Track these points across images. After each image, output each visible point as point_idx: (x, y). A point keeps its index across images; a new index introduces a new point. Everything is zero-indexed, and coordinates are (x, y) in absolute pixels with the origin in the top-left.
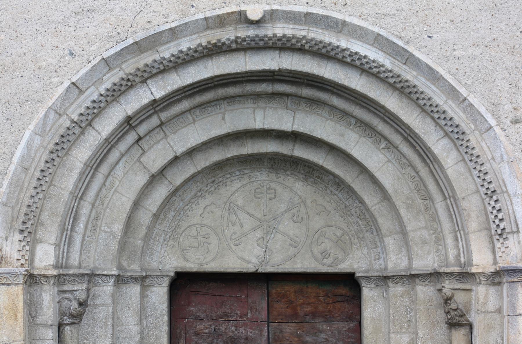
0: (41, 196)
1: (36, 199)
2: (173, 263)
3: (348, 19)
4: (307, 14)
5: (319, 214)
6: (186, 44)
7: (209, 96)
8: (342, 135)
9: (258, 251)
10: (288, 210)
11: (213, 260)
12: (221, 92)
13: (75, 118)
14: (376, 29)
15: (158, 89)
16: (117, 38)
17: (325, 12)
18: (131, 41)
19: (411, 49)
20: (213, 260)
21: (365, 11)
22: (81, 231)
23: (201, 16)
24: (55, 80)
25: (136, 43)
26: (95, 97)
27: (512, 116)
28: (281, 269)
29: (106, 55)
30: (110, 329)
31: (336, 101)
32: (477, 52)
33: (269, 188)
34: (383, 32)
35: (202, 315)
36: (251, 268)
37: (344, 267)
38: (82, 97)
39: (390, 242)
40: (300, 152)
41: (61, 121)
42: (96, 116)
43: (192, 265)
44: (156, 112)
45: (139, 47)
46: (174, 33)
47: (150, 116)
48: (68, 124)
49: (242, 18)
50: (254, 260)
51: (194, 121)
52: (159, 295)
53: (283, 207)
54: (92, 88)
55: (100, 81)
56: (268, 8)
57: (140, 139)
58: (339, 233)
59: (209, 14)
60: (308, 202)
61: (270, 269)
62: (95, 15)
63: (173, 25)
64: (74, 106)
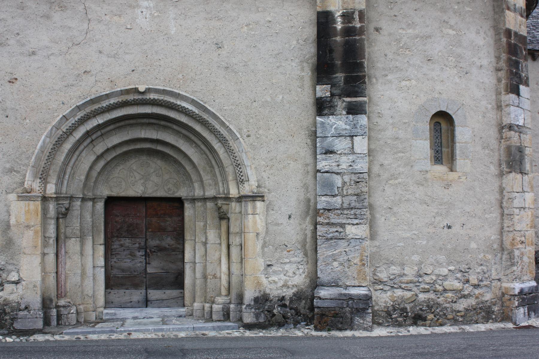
0: (49, 163)
1: (47, 165)
2: (106, 193)
3: (181, 93)
4: (164, 90)
5: (167, 173)
6: (112, 101)
7: (122, 123)
8: (177, 141)
9: (142, 188)
10: (154, 172)
11: (123, 192)
12: (127, 122)
13: (65, 131)
14: (192, 97)
15: (100, 120)
16: (83, 97)
17: (171, 90)
18: (89, 99)
19: (206, 105)
20: (123, 192)
21: (188, 89)
22: (67, 179)
23: (119, 89)
24: (56, 114)
25: (91, 100)
26: (73, 122)
27: (247, 134)
28: (151, 196)
29: (78, 104)
30: (79, 220)
31: (175, 127)
32: (233, 108)
33: (147, 163)
34: (195, 98)
35: (118, 214)
36: (139, 195)
37: (177, 195)
38: (68, 122)
39: (196, 185)
40: (160, 148)
41: (58, 132)
42: (74, 130)
43: (114, 194)
44: (99, 130)
45: (92, 102)
46: (108, 96)
47: (97, 131)
48: (61, 133)
49: (136, 91)
50: (140, 192)
51: (116, 134)
52: (100, 206)
53: (152, 170)
54: (72, 118)
55: (75, 115)
56: (147, 87)
57: (93, 141)
58: (175, 181)
59: (122, 89)
60: (163, 168)
61: (147, 196)
62: (74, 87)
63: (107, 93)
64: (64, 126)
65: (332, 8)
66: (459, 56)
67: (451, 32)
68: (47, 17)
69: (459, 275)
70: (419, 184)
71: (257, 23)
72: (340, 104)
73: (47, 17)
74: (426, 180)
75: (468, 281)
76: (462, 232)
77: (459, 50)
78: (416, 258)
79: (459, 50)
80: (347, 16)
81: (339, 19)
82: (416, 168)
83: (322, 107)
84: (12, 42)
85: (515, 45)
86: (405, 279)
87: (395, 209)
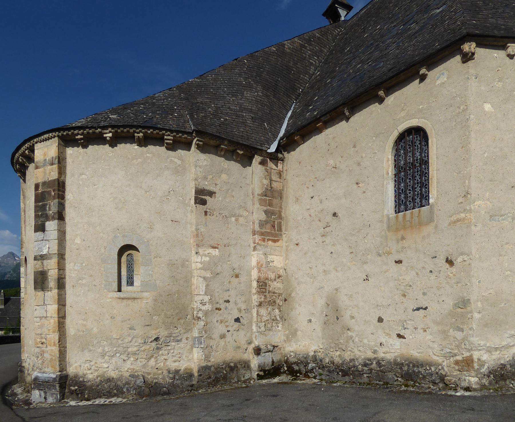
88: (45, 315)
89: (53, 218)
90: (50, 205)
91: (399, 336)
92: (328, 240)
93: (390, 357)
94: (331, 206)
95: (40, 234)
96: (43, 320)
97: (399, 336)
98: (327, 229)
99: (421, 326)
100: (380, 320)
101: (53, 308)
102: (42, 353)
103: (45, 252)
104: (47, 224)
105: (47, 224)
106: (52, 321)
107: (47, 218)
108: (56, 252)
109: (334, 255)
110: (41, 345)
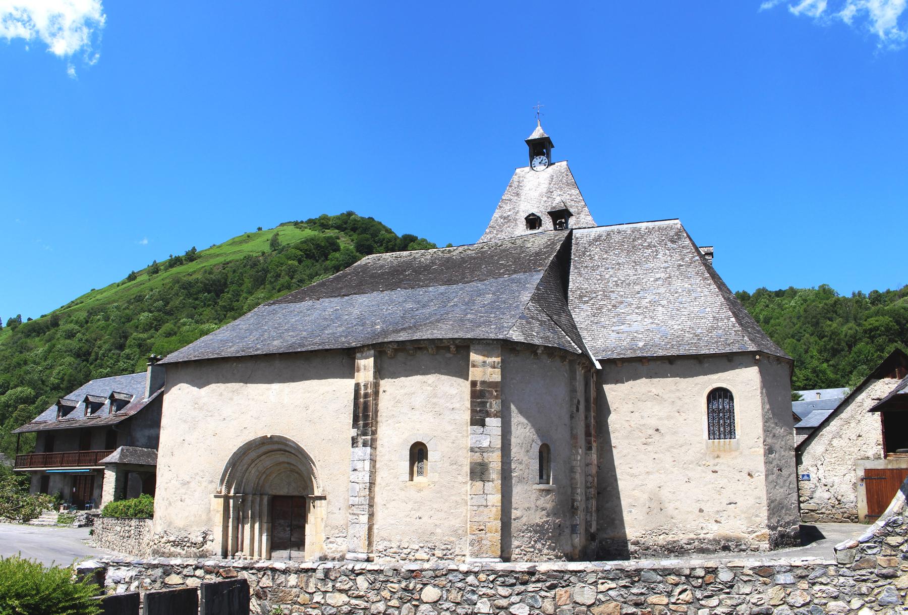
52: (266, 499)
65: (360, 381)
66: (435, 404)
67: (429, 388)
68: (231, 399)
69: (427, 550)
70: (402, 489)
71: (328, 392)
72: (360, 440)
73: (231, 399)
74: (406, 487)
75: (434, 555)
76: (430, 521)
77: (435, 400)
78: (399, 537)
79: (435, 400)
80: (366, 386)
81: (362, 388)
82: (400, 479)
83: (354, 441)
84: (216, 414)
85: (481, 391)
86: (392, 550)
87: (388, 505)
88: (485, 504)
89: (496, 416)
90: (491, 403)
91: (716, 521)
92: (650, 448)
93: (710, 536)
94: (654, 422)
95: (479, 429)
96: (482, 509)
97: (716, 521)
98: (650, 440)
99: (732, 515)
100: (701, 511)
101: (495, 499)
102: (480, 541)
103: (485, 444)
104: (487, 419)
105: (487, 419)
106: (494, 509)
107: (488, 415)
108: (500, 446)
109: (656, 461)
110: (478, 532)
